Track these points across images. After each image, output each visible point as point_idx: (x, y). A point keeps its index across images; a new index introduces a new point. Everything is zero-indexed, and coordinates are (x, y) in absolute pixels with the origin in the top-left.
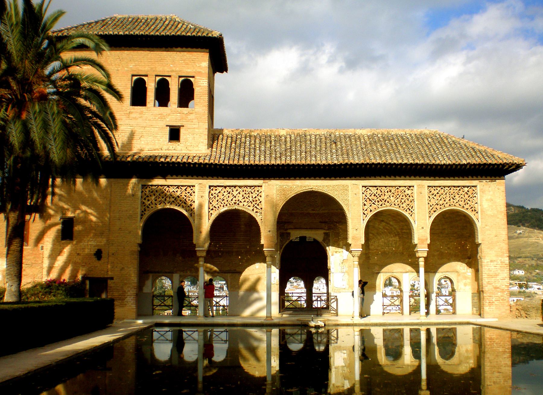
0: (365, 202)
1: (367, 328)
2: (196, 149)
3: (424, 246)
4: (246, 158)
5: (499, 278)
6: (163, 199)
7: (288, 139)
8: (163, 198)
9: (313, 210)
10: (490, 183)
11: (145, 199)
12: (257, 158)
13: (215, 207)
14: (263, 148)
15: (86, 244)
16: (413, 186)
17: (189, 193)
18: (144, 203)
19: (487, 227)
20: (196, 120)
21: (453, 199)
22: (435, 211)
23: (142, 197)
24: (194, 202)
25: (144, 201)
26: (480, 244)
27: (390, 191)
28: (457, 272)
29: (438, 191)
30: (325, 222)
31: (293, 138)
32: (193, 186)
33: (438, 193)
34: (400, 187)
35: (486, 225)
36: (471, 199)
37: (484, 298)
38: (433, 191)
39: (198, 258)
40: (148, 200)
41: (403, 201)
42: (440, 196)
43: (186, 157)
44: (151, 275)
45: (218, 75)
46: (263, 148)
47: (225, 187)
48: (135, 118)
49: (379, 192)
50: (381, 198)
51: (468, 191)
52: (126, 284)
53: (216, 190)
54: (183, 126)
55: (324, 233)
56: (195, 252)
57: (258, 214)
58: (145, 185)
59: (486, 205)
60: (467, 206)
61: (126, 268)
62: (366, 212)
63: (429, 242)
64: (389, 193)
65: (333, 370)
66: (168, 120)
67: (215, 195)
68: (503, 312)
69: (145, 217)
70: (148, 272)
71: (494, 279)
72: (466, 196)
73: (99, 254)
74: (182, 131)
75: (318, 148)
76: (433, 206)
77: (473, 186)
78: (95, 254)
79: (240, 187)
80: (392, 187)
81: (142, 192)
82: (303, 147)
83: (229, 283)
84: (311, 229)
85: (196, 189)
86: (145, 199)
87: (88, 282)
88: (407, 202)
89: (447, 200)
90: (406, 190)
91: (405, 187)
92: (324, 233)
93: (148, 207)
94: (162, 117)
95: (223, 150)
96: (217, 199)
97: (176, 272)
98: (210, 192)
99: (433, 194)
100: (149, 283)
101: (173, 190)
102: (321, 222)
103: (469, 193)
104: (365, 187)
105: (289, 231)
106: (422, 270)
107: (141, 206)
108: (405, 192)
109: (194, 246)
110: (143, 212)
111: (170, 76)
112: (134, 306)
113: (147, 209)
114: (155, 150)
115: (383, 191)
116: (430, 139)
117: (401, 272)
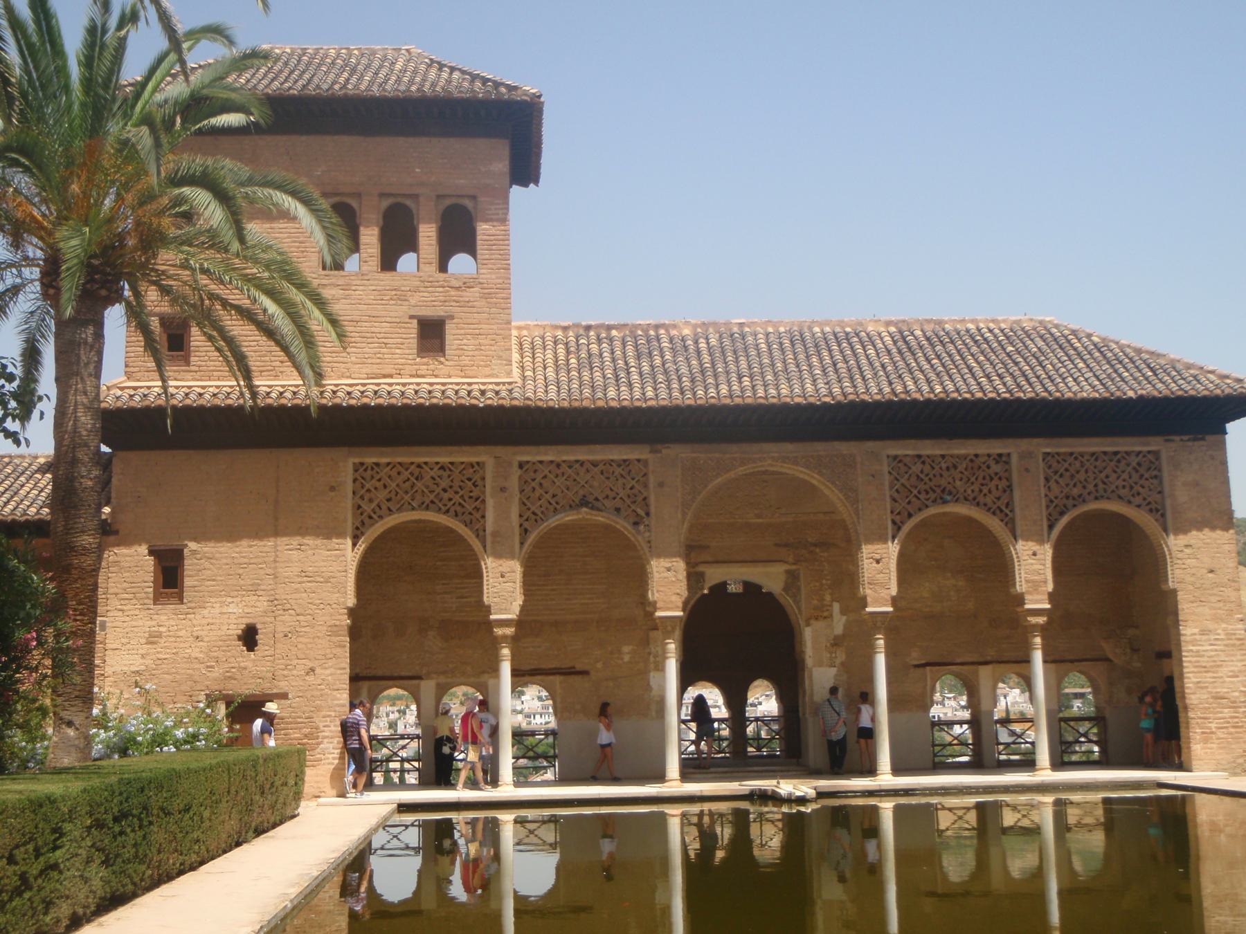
0: (896, 495)
1: (872, 801)
2: (487, 371)
3: (1039, 597)
4: (612, 393)
5: (1223, 671)
6: (407, 497)
7: (703, 345)
8: (407, 492)
9: (758, 516)
10: (1190, 444)
11: (362, 498)
12: (637, 395)
13: (534, 513)
14: (646, 368)
15: (218, 611)
16: (1009, 455)
17: (469, 479)
18: (359, 507)
19: (1187, 551)
20: (483, 303)
21: (1104, 483)
22: (1062, 514)
23: (354, 493)
24: (484, 501)
25: (360, 503)
26: (1174, 592)
27: (955, 467)
28: (1108, 660)
29: (1066, 465)
30: (786, 545)
31: (713, 342)
32: (478, 463)
33: (1067, 470)
34: (976, 456)
35: (1186, 546)
36: (1146, 484)
37: (1188, 723)
38: (1055, 464)
40: (371, 501)
41: (985, 490)
42: (1072, 476)
43: (463, 393)
45: (516, 190)
46: (646, 368)
47: (558, 465)
49: (927, 468)
50: (932, 484)
51: (1139, 464)
52: (318, 709)
53: (535, 471)
54: (452, 317)
55: (788, 572)
56: (490, 625)
57: (642, 527)
58: (362, 464)
59: (1182, 495)
60: (1138, 500)
61: (318, 671)
62: (898, 519)
63: (1050, 587)
64: (952, 471)
65: (819, 903)
66: (413, 302)
67: (533, 484)
68: (1238, 757)
71: (1210, 675)
72: (1135, 477)
73: (249, 638)
74: (450, 330)
75: (779, 365)
76: (1056, 502)
77: (1149, 452)
78: (240, 638)
79: (595, 464)
80: (958, 456)
81: (355, 480)
82: (743, 364)
83: (558, 700)
84: (754, 561)
86: (362, 498)
87: (222, 710)
88: (996, 493)
89: (1090, 487)
90: (992, 463)
91: (989, 456)
92: (788, 572)
93: (370, 517)
95: (551, 373)
96: (539, 492)
97: (428, 676)
98: (520, 477)
99: (1056, 473)
101: (432, 473)
102: (776, 545)
103: (1142, 470)
104: (895, 457)
105: (701, 568)
106: (1038, 657)
107: (354, 515)
108: (988, 467)
109: (488, 610)
110: (357, 528)
111: (415, 197)
113: (367, 521)
114: (385, 376)
115: (937, 468)
116: (1041, 343)
117: (973, 663)
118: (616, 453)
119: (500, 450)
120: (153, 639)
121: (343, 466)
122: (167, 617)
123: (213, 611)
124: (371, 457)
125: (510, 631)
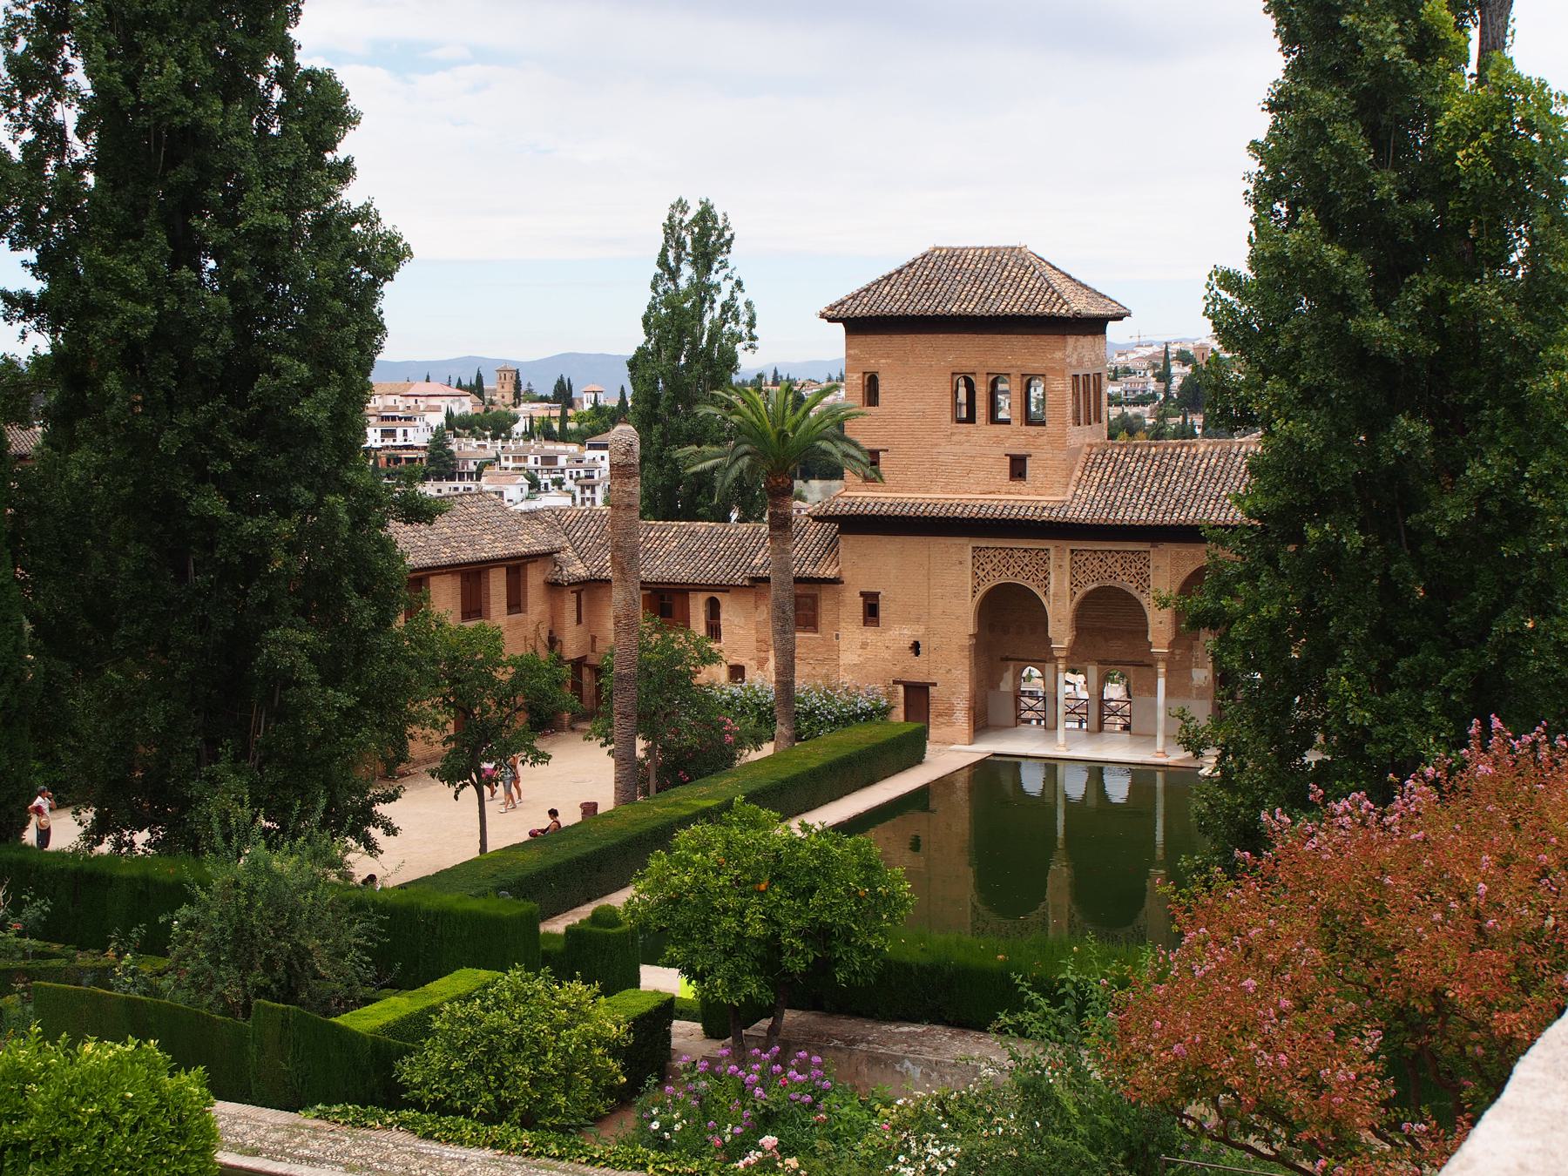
39: (1057, 659)
44: (1012, 665)
48: (960, 443)
69: (979, 596)
70: (1007, 659)
73: (916, 648)
74: (1029, 461)
85: (1052, 554)
87: (901, 688)
94: (999, 441)
100: (1008, 677)
112: (966, 726)
118: (1131, 546)
119: (1057, 543)
120: (864, 646)
121: (964, 548)
122: (870, 634)
123: (895, 632)
124: (983, 543)
125: (1064, 654)
